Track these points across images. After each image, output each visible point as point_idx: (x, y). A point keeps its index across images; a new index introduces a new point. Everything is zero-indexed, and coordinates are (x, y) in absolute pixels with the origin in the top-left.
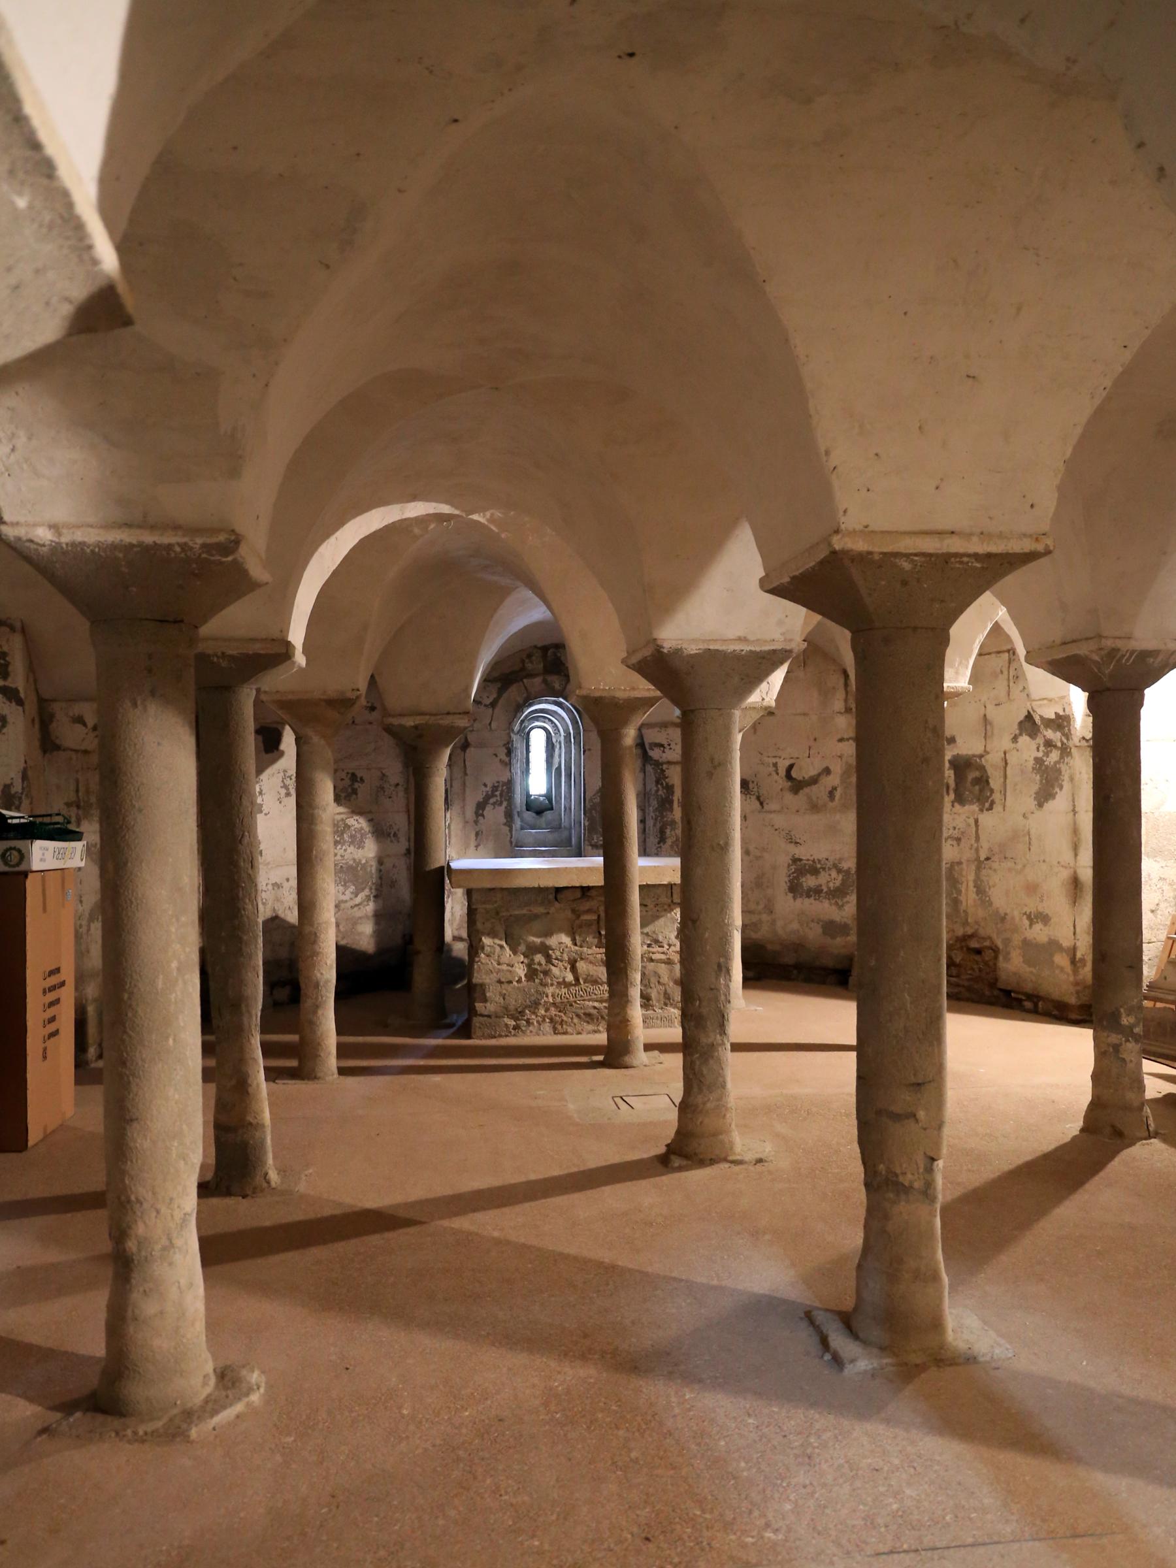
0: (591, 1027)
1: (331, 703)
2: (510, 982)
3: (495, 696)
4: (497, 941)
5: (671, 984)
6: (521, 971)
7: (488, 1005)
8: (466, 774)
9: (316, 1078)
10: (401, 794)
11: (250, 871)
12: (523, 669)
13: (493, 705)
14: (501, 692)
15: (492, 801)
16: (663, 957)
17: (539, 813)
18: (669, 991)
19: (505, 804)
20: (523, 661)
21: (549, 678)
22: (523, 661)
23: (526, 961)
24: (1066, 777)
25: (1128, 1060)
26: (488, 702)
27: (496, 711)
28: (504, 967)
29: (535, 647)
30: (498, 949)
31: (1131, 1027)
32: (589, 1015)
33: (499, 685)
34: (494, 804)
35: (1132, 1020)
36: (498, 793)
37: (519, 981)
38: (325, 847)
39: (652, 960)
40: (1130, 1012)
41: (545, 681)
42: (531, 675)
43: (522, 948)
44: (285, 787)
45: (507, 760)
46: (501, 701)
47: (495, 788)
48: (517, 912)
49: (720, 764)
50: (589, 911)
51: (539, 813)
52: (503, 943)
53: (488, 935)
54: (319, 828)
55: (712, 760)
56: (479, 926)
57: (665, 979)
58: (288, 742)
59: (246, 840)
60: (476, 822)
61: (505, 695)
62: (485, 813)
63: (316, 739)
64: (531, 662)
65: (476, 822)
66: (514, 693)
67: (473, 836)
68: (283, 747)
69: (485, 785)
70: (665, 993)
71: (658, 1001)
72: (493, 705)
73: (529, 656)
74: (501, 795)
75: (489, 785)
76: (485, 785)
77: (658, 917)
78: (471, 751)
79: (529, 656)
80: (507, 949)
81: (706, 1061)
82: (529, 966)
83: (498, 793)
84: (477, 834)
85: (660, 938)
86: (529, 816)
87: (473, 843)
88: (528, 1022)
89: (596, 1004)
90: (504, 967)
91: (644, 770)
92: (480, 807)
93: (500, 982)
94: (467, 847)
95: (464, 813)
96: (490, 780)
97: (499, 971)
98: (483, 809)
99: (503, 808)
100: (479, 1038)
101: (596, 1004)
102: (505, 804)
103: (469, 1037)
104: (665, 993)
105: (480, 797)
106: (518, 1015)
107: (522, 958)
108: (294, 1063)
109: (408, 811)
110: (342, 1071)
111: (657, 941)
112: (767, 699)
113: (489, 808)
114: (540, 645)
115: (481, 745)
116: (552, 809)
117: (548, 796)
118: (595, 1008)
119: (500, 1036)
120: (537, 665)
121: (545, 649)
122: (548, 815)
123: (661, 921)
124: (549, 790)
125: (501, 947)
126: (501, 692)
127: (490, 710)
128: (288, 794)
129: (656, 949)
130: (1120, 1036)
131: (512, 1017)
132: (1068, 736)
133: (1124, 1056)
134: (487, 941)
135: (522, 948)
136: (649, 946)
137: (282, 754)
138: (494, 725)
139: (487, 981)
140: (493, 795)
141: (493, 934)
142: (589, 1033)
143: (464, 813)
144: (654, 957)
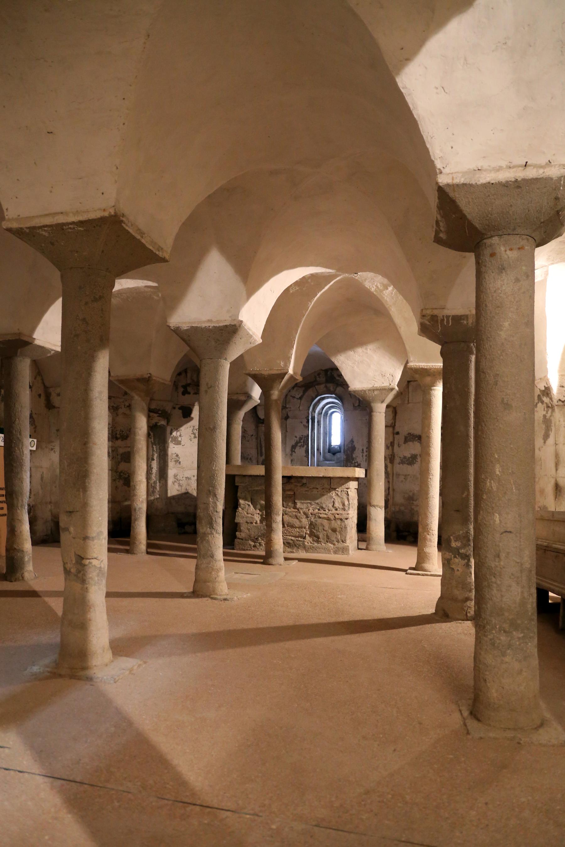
0: (289, 550)
1: (138, 380)
2: (252, 523)
3: (301, 394)
4: (247, 502)
5: (330, 531)
6: (257, 518)
7: (242, 533)
8: (287, 431)
9: (134, 554)
10: (254, 440)
11: (19, 436)
12: (316, 381)
13: (301, 398)
14: (304, 392)
15: (299, 444)
16: (325, 516)
17: (334, 454)
18: (329, 534)
19: (305, 446)
20: (315, 377)
22: (315, 377)
23: (260, 513)
24: (553, 422)
25: (456, 569)
27: (302, 401)
28: (250, 515)
30: (247, 506)
31: (458, 549)
32: (288, 543)
33: (303, 389)
34: (300, 446)
35: (458, 544)
36: (302, 441)
37: (256, 523)
38: (140, 446)
39: (320, 518)
40: (457, 539)
41: (326, 387)
42: (319, 384)
43: (258, 506)
44: (194, 434)
45: (307, 425)
46: (305, 396)
47: (301, 439)
48: (256, 488)
49: (211, 387)
50: (290, 490)
51: (334, 454)
52: (250, 503)
53: (243, 499)
54: (137, 437)
55: (207, 384)
56: (239, 494)
57: (327, 528)
58: (195, 413)
59: (17, 422)
60: (291, 455)
61: (306, 394)
62: (296, 451)
63: (136, 397)
64: (320, 377)
65: (291, 455)
66: (310, 392)
67: (290, 461)
68: (193, 415)
69: (296, 437)
70: (327, 536)
71: (324, 539)
72: (301, 398)
73: (319, 374)
74: (304, 442)
75: (298, 437)
76: (296, 437)
77: (323, 495)
78: (289, 421)
79: (319, 374)
80: (252, 507)
81: (202, 542)
82: (261, 516)
83: (302, 441)
84: (292, 461)
85: (324, 506)
86: (329, 455)
88: (260, 543)
89: (293, 538)
90: (250, 515)
92: (293, 447)
93: (247, 522)
96: (298, 435)
97: (247, 517)
98: (295, 449)
100: (237, 550)
101: (293, 538)
102: (305, 446)
103: (233, 549)
104: (327, 536)
105: (293, 443)
106: (255, 540)
107: (258, 511)
108: (128, 548)
109: (257, 448)
110: (148, 553)
111: (322, 508)
112: (392, 385)
113: (298, 448)
114: (323, 369)
115: (295, 417)
117: (340, 446)
118: (292, 540)
119: (247, 550)
120: (323, 379)
121: (326, 371)
123: (324, 498)
125: (249, 505)
126: (304, 392)
127: (299, 401)
128: (195, 437)
129: (322, 511)
130: (451, 554)
131: (253, 541)
132: (551, 399)
133: (453, 567)
134: (241, 501)
135: (258, 506)
136: (319, 510)
137: (192, 419)
138: (301, 408)
139: (241, 521)
140: (300, 442)
141: (245, 499)
142: (289, 553)
144: (321, 516)
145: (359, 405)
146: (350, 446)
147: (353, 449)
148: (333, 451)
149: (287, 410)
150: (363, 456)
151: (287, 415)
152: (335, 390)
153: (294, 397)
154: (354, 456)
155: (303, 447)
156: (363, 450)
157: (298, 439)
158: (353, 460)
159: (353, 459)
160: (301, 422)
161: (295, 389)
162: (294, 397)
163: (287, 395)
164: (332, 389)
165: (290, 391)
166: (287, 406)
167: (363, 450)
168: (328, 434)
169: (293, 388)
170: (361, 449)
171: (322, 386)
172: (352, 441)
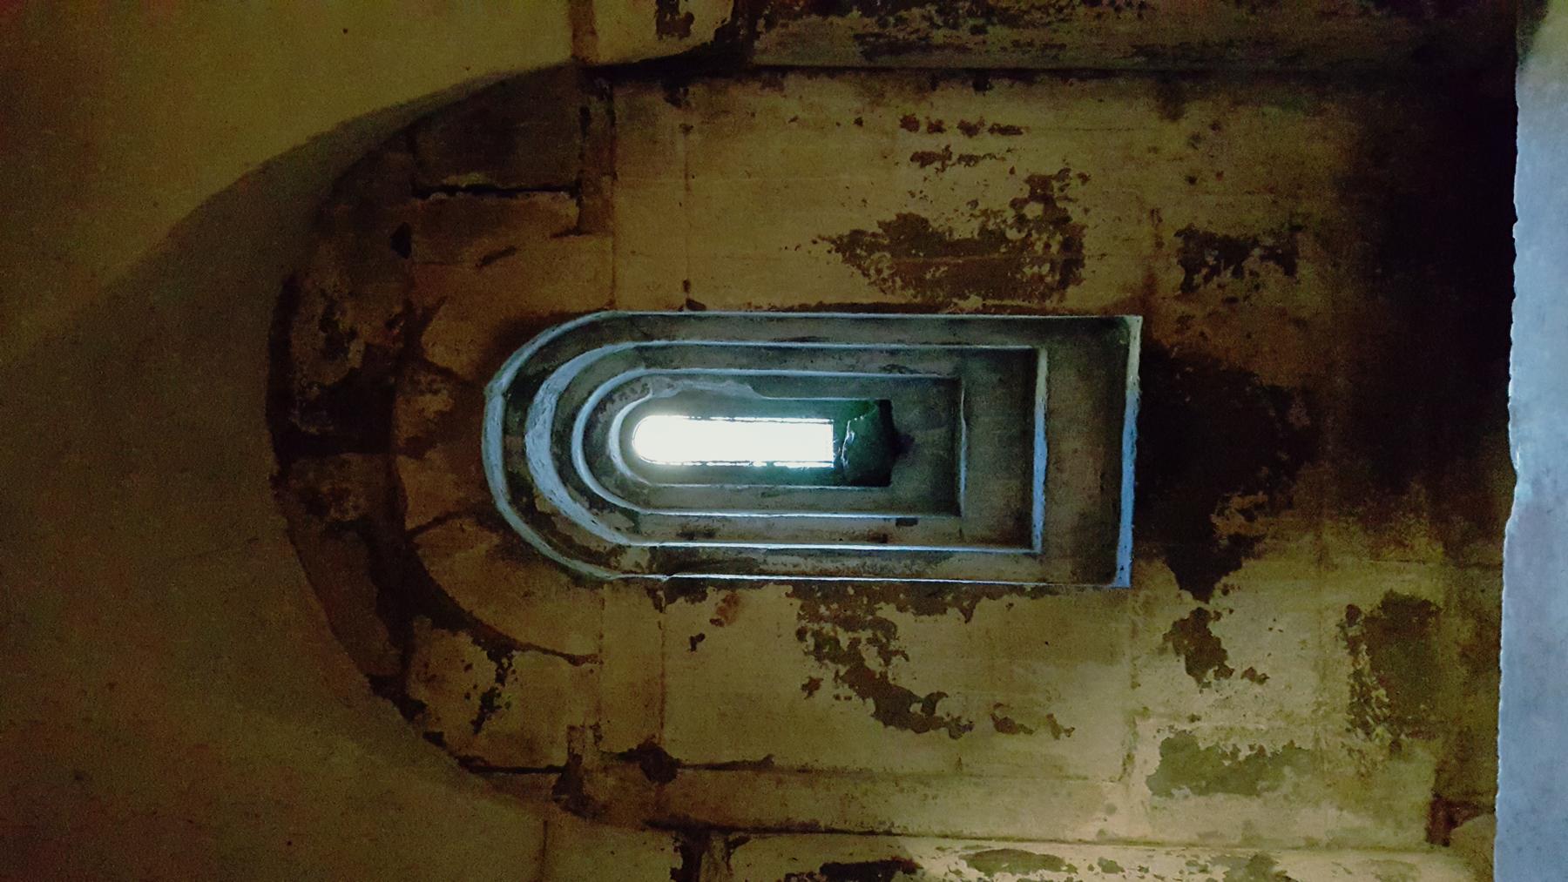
3: (464, 639)
8: (765, 765)
13: (500, 647)
14: (453, 619)
15: (873, 662)
19: (887, 611)
21: (405, 428)
26: (485, 672)
29: (278, 481)
34: (886, 655)
36: (844, 639)
41: (417, 449)
45: (715, 598)
46: (486, 614)
47: (824, 649)
60: (958, 728)
61: (466, 602)
64: (339, 496)
65: (958, 728)
66: (459, 568)
69: (812, 686)
72: (500, 647)
73: (314, 504)
74: (849, 624)
75: (812, 668)
76: (812, 686)
79: (314, 504)
84: (1004, 726)
87: (1042, 745)
91: (774, 75)
92: (896, 709)
94: (1057, 771)
95: (923, 780)
96: (795, 665)
98: (910, 697)
99: (906, 623)
102: (887, 611)
113: (904, 676)
115: (655, 700)
116: (885, 406)
121: (288, 445)
122: (908, 417)
124: (821, 411)
126: (453, 619)
138: (578, 645)
143: (923, 780)
145: (575, 190)
146: (885, 259)
147: (911, 235)
148: (873, 462)
149: (589, 759)
150: (970, 160)
151: (628, 757)
152: (446, 373)
153: (489, 702)
154: (966, 229)
155: (889, 628)
156: (923, 159)
157: (826, 673)
158: (1002, 238)
159: (991, 238)
160: (696, 641)
161: (421, 693)
162: (489, 702)
163: (468, 763)
164: (435, 403)
165: (436, 739)
166: (559, 758)
167: (923, 159)
168: (771, 485)
169: (412, 710)
170: (910, 175)
171: (410, 473)
172: (851, 246)
